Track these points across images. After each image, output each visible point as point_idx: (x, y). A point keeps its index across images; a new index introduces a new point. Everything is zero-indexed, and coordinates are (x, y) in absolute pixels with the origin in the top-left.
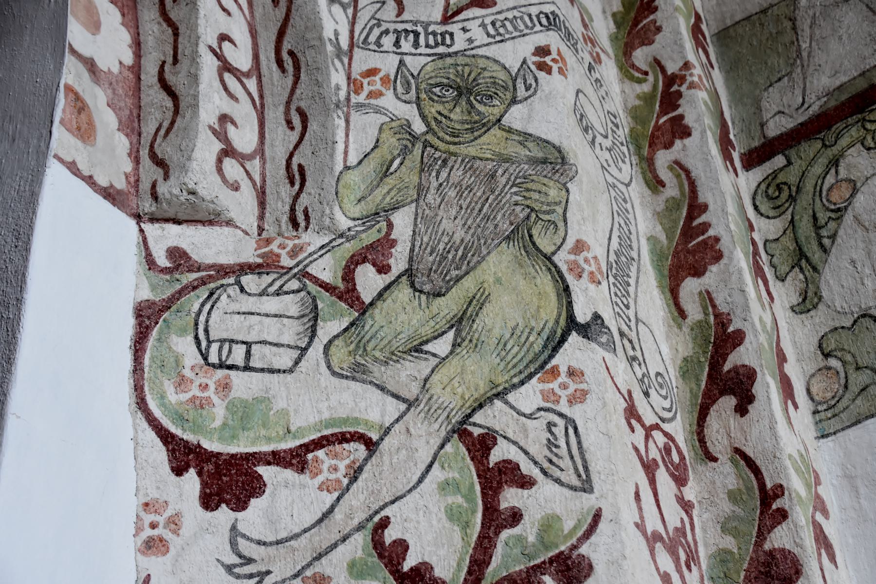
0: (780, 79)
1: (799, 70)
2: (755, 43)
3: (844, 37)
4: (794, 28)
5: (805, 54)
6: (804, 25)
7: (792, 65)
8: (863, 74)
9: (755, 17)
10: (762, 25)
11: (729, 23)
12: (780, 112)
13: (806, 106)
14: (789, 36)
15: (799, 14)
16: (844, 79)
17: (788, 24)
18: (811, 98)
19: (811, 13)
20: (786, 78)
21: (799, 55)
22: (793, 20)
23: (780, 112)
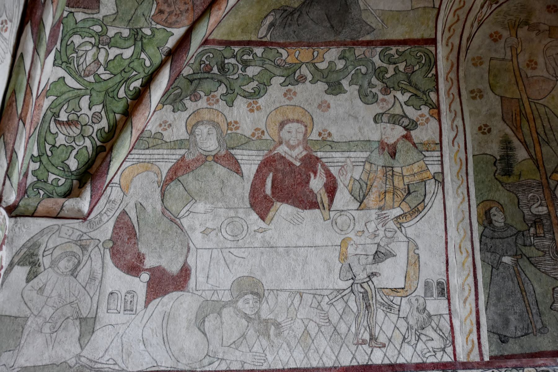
0: (10, 351)
1: (17, 351)
2: (8, 329)
3: (35, 347)
4: (22, 332)
5: (21, 346)
6: (26, 333)
7: (16, 347)
8: (34, 366)
9: (12, 318)
10: (13, 323)
11: (3, 314)
12: (5, 365)
13: (13, 368)
14: (19, 335)
15: (26, 327)
16: (28, 365)
17: (21, 329)
18: (16, 366)
19: (29, 329)
20: (12, 352)
21: (19, 345)
22: (23, 328)
23: (5, 365)
